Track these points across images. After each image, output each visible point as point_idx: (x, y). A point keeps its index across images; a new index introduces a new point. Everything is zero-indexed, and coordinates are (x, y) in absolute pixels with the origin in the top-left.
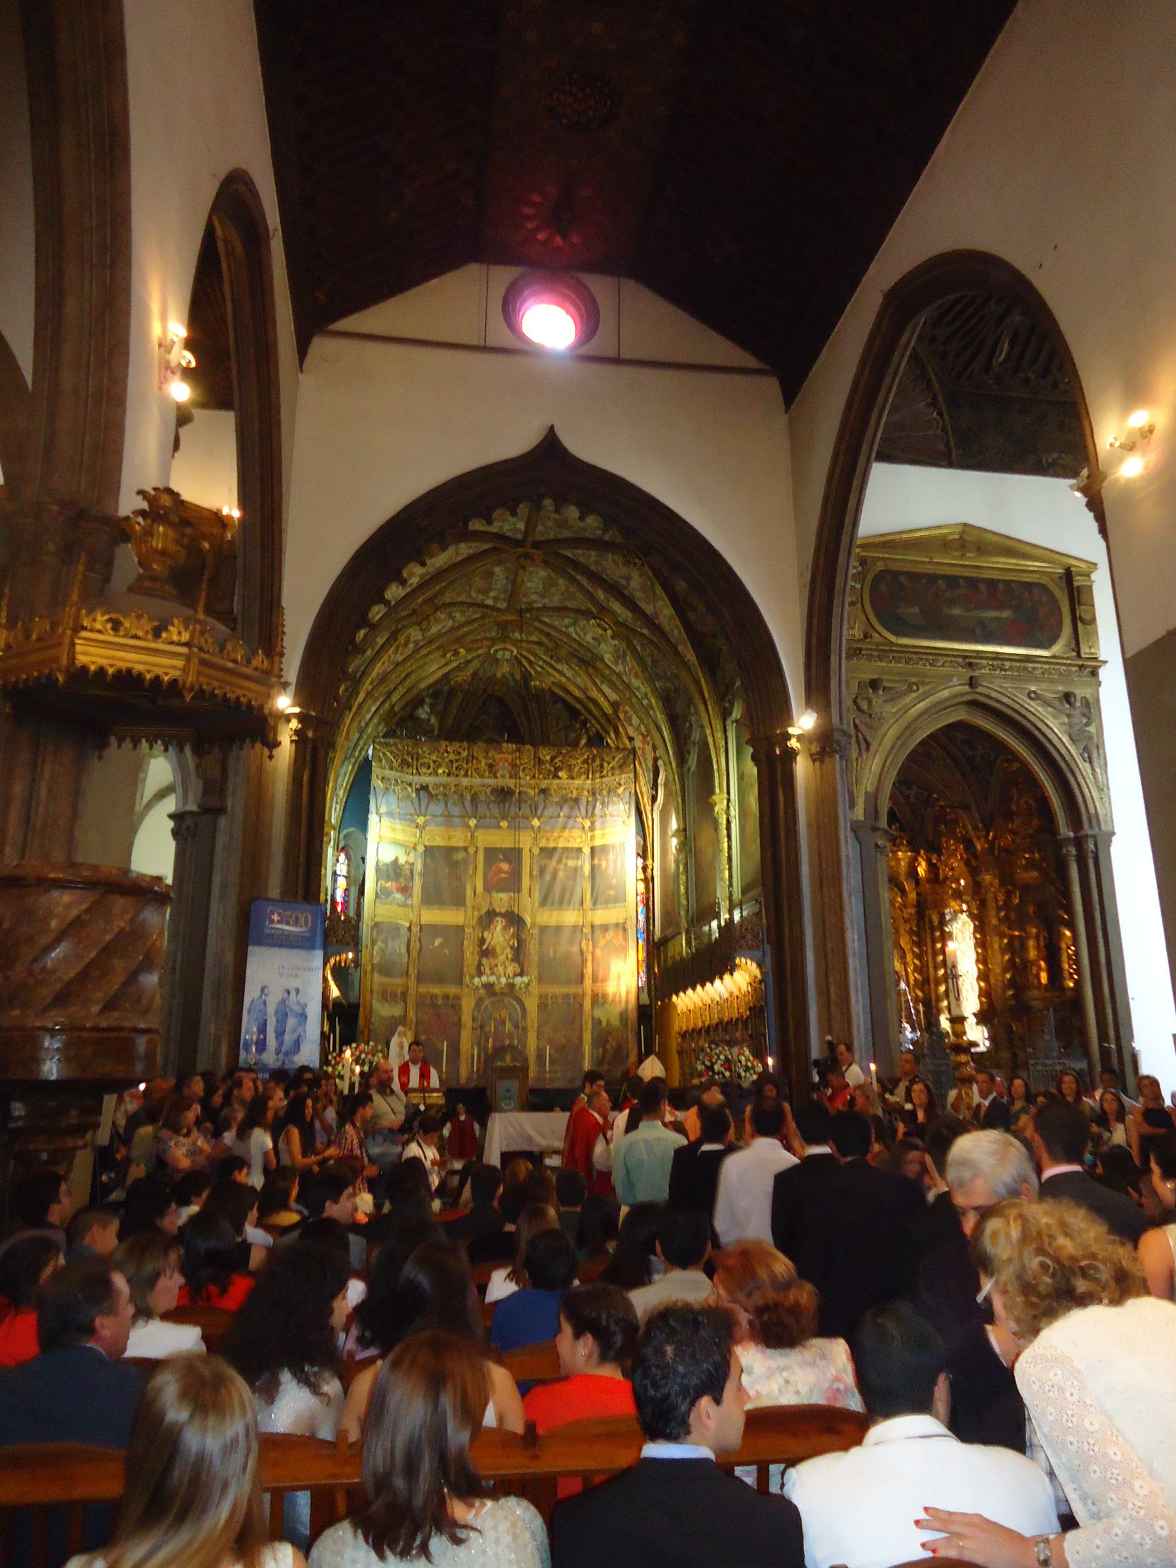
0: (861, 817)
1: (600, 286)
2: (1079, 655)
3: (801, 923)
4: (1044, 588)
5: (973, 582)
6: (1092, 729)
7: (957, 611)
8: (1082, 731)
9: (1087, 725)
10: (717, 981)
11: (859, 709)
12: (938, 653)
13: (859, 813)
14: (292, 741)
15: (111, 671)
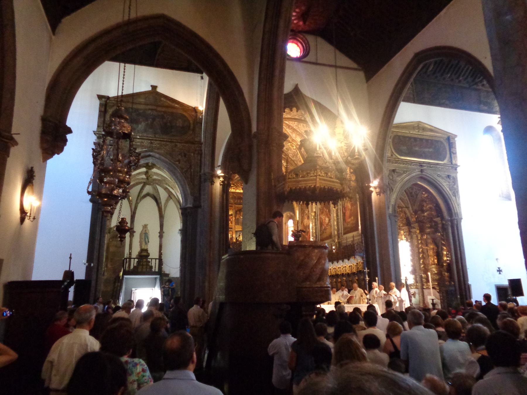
0: (391, 212)
1: (311, 39)
2: (452, 163)
3: (375, 244)
4: (442, 143)
5: (421, 140)
6: (455, 186)
7: (417, 149)
8: (453, 187)
9: (454, 185)
10: (341, 262)
11: (390, 179)
12: (411, 162)
13: (391, 211)
14: (220, 185)
15: (326, 187)
